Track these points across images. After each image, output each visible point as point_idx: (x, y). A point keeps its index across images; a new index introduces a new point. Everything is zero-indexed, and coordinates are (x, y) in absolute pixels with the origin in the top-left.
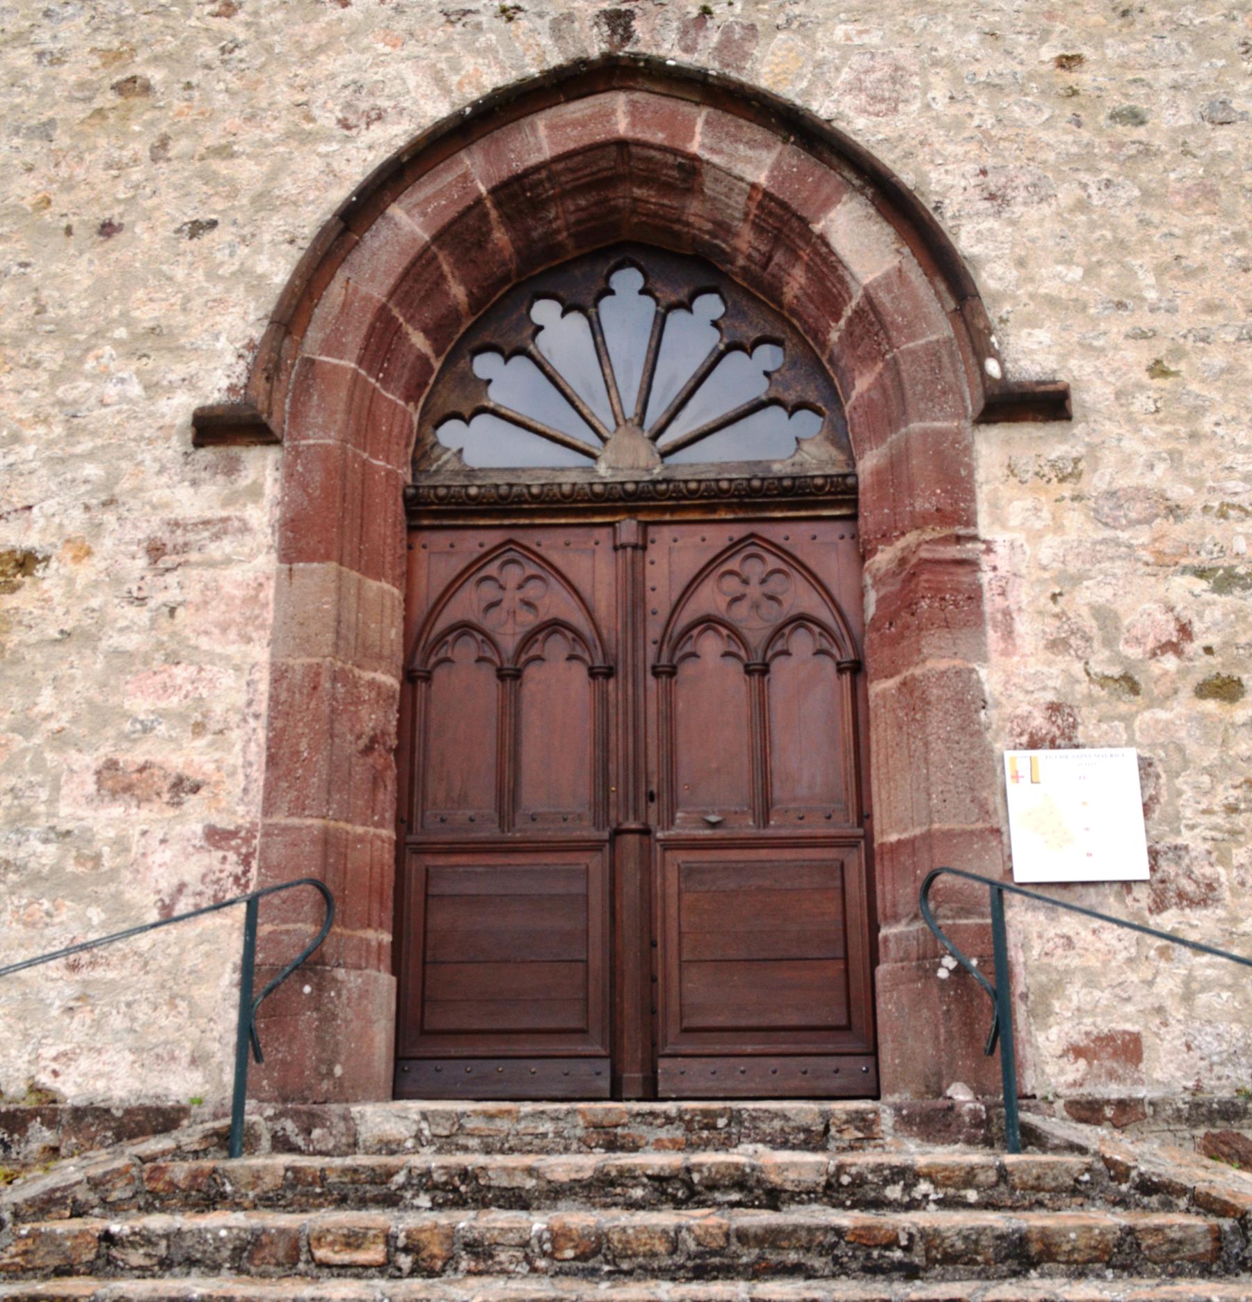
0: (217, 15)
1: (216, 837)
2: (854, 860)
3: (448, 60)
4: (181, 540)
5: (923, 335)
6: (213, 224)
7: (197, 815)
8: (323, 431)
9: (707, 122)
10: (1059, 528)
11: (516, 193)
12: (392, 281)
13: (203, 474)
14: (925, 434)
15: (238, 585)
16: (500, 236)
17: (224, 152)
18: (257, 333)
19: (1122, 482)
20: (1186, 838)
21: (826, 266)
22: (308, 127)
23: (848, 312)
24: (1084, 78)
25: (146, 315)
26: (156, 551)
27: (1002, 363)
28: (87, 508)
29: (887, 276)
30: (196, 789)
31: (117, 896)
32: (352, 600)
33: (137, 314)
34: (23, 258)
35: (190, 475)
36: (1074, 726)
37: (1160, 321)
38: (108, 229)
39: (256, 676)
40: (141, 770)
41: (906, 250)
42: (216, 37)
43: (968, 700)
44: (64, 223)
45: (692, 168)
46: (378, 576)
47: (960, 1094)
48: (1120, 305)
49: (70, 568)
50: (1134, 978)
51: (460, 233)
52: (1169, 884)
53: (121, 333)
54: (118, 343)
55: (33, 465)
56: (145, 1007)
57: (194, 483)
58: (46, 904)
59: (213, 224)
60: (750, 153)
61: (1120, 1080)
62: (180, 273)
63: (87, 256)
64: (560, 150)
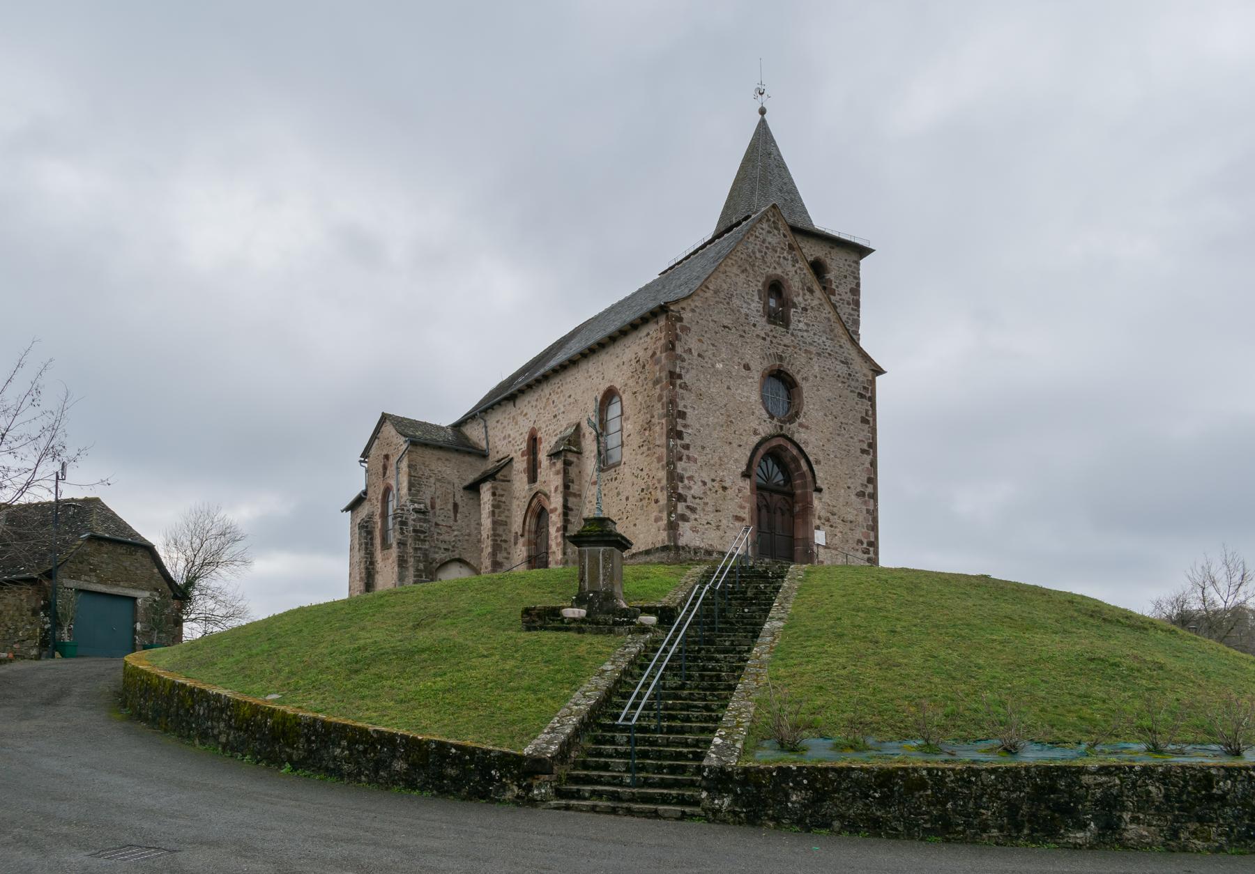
21: (799, 467)
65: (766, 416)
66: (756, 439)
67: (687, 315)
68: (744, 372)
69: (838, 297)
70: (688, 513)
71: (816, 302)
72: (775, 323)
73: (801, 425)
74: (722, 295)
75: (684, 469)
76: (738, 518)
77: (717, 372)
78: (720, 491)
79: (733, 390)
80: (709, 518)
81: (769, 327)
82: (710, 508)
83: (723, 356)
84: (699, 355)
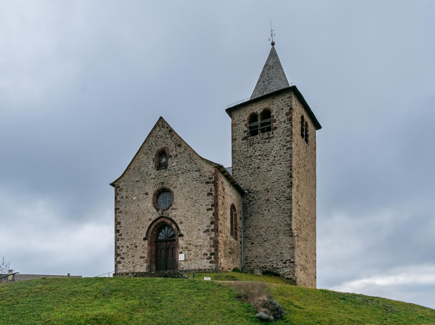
52: (185, 260)
65: (155, 210)
66: (150, 222)
67: (121, 185)
69: (278, 122)
70: (121, 260)
71: (183, 149)
72: (160, 169)
73: (173, 209)
74: (136, 169)
75: (120, 244)
77: (134, 201)
78: (134, 248)
80: (129, 260)
81: (157, 172)
82: (130, 256)
84: (126, 197)
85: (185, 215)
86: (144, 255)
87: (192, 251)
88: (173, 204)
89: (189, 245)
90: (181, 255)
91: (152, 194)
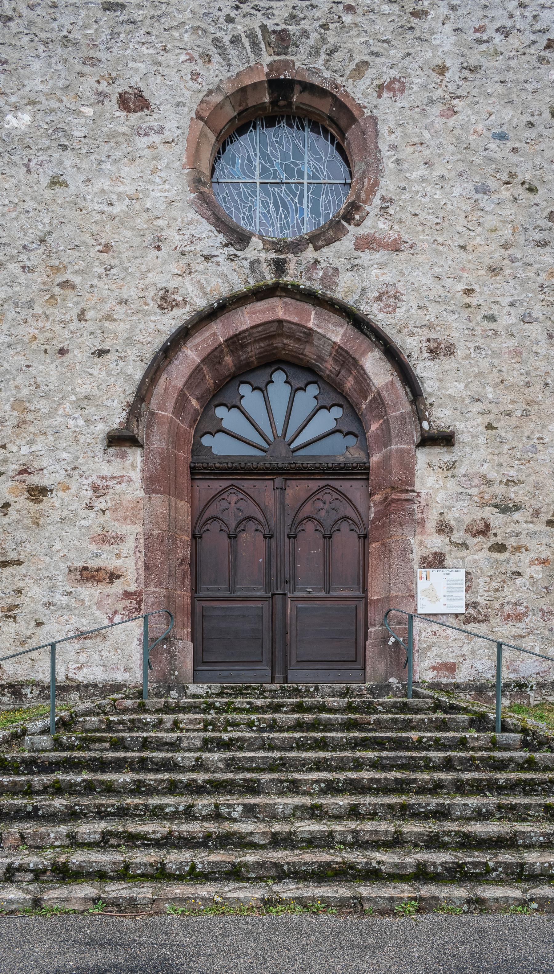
0: (102, 252)
1: (127, 595)
2: (361, 605)
3: (206, 279)
4: (105, 484)
5: (399, 410)
6: (108, 351)
7: (118, 587)
8: (158, 441)
9: (316, 313)
10: (445, 487)
11: (235, 342)
12: (185, 379)
13: (112, 458)
14: (397, 450)
15: (129, 502)
16: (228, 359)
17: (109, 318)
18: (131, 399)
19: (470, 471)
20: (479, 599)
21: (362, 378)
22: (146, 308)
23: (370, 397)
24: (474, 300)
25: (83, 390)
26: (95, 488)
27: (429, 423)
28: (66, 470)
29: (387, 384)
30: (118, 577)
31: (92, 615)
32: (173, 508)
33: (77, 390)
34: (27, 363)
35: (106, 458)
36: (443, 560)
37: (492, 407)
38: (62, 352)
39: (139, 537)
40: (97, 570)
41: (395, 374)
42: (102, 263)
43: (407, 551)
44: (43, 348)
45: (309, 333)
46: (182, 499)
47: (392, 680)
48: (478, 400)
49: (61, 494)
50: (457, 645)
51: (212, 359)
52: (472, 615)
53: (73, 398)
54: (72, 402)
55: (41, 453)
56: (106, 652)
57: (108, 461)
58: (66, 617)
59: (108, 351)
60: (334, 328)
61: (448, 677)
62: (95, 372)
63: (54, 364)
64: (254, 324)
65: (210, 238)
68: (122, 121)
76: (88, 575)
79: (75, 183)
83: (35, 84)
85: (474, 300)
86: (107, 560)
87: (526, 557)
88: (372, 208)
89: (504, 509)
90: (435, 574)
91: (188, 114)
